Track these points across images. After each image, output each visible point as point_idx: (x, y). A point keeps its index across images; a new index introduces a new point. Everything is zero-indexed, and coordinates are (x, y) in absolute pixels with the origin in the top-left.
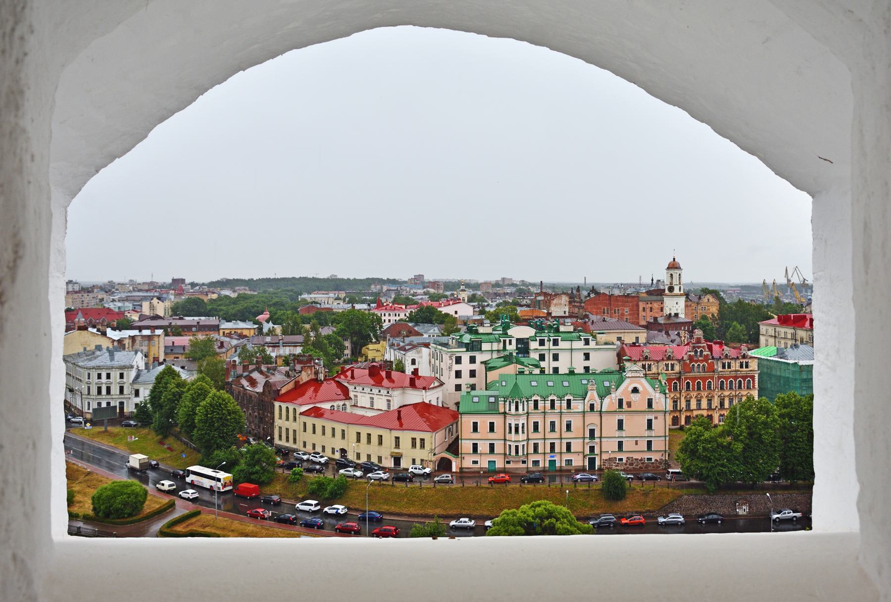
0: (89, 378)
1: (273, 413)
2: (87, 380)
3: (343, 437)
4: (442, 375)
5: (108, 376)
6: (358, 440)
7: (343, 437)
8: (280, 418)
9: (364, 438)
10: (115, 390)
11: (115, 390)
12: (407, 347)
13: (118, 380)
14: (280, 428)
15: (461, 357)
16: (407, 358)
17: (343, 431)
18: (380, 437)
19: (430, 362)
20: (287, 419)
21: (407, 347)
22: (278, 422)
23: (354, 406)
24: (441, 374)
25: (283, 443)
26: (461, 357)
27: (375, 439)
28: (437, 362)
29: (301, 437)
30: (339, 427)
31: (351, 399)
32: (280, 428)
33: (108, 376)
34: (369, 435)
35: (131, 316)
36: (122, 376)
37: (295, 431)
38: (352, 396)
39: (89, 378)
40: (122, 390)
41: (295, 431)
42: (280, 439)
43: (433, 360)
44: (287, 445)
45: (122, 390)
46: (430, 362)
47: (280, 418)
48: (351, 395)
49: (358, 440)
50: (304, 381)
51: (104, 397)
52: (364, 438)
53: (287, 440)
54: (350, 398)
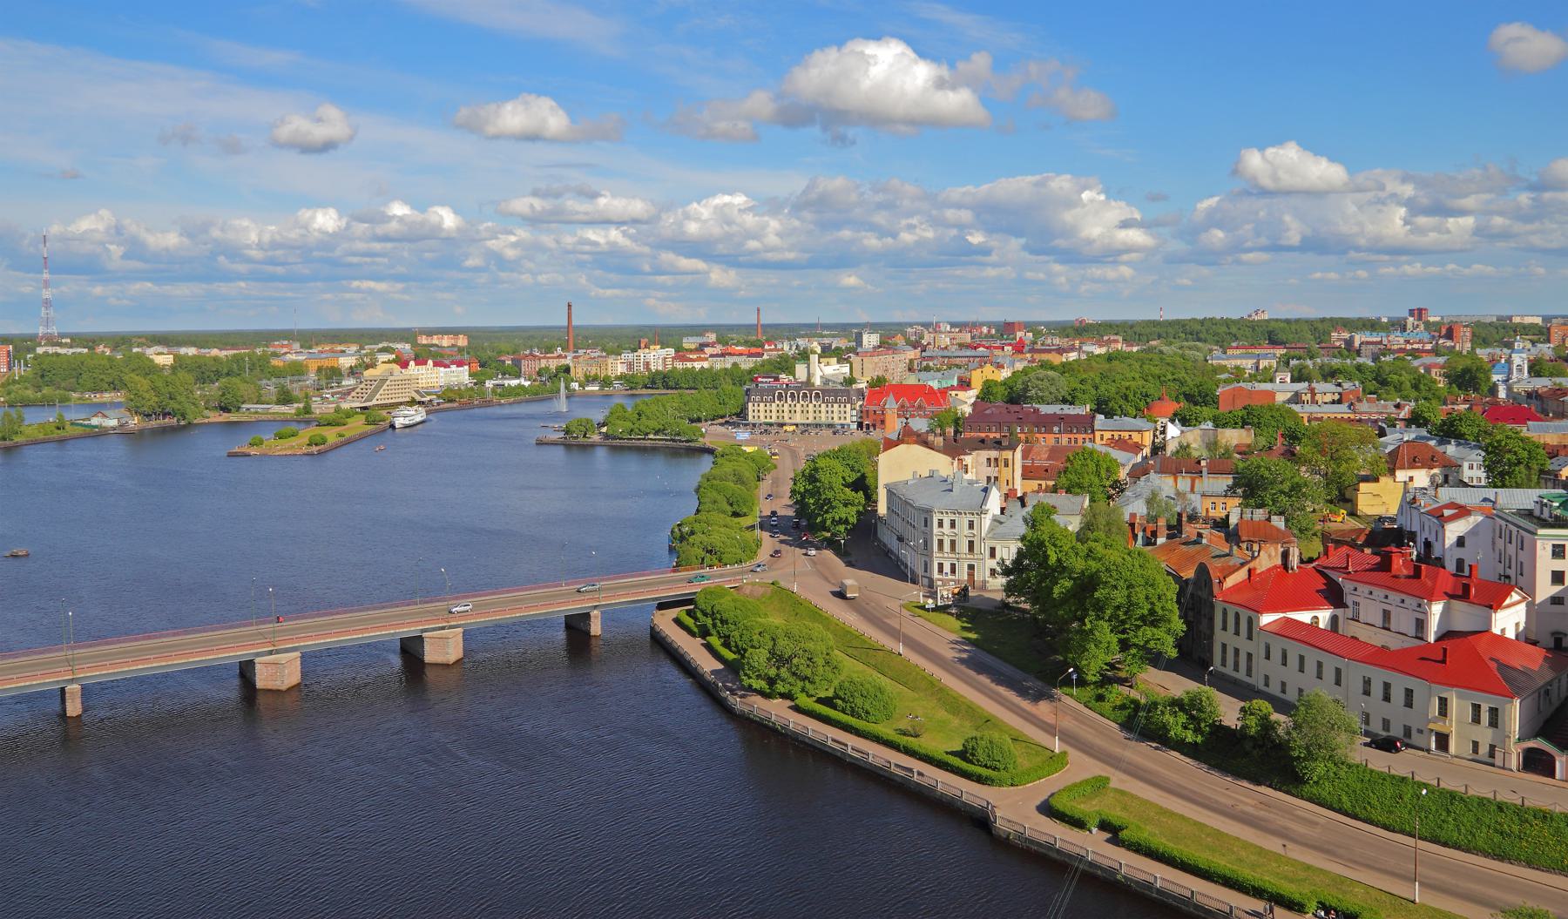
0: (926, 526)
1: (1211, 619)
2: (923, 528)
3: (1338, 682)
4: (1522, 574)
5: (953, 524)
6: (1367, 693)
7: (1338, 682)
8: (1225, 628)
9: (1377, 690)
10: (963, 546)
11: (963, 546)
12: (1447, 513)
13: (966, 531)
14: (1224, 646)
15: (1564, 546)
16: (1448, 534)
17: (1338, 671)
18: (1409, 693)
19: (1494, 543)
20: (1237, 633)
21: (1447, 513)
22: (1220, 637)
23: (1353, 619)
24: (1519, 572)
25: (1229, 670)
26: (1564, 546)
27: (1398, 695)
28: (1511, 549)
29: (1261, 667)
30: (1331, 663)
31: (1347, 607)
32: (1224, 646)
33: (953, 524)
34: (1387, 686)
35: (956, 395)
36: (971, 525)
37: (1250, 656)
38: (1350, 603)
39: (926, 526)
40: (971, 544)
41: (1250, 656)
42: (1224, 664)
43: (1500, 543)
44: (1234, 674)
45: (971, 544)
46: (1494, 543)
47: (1225, 628)
48: (1349, 600)
49: (1367, 693)
50: (1263, 569)
51: (946, 555)
52: (1377, 690)
53: (1236, 668)
54: (1345, 606)
